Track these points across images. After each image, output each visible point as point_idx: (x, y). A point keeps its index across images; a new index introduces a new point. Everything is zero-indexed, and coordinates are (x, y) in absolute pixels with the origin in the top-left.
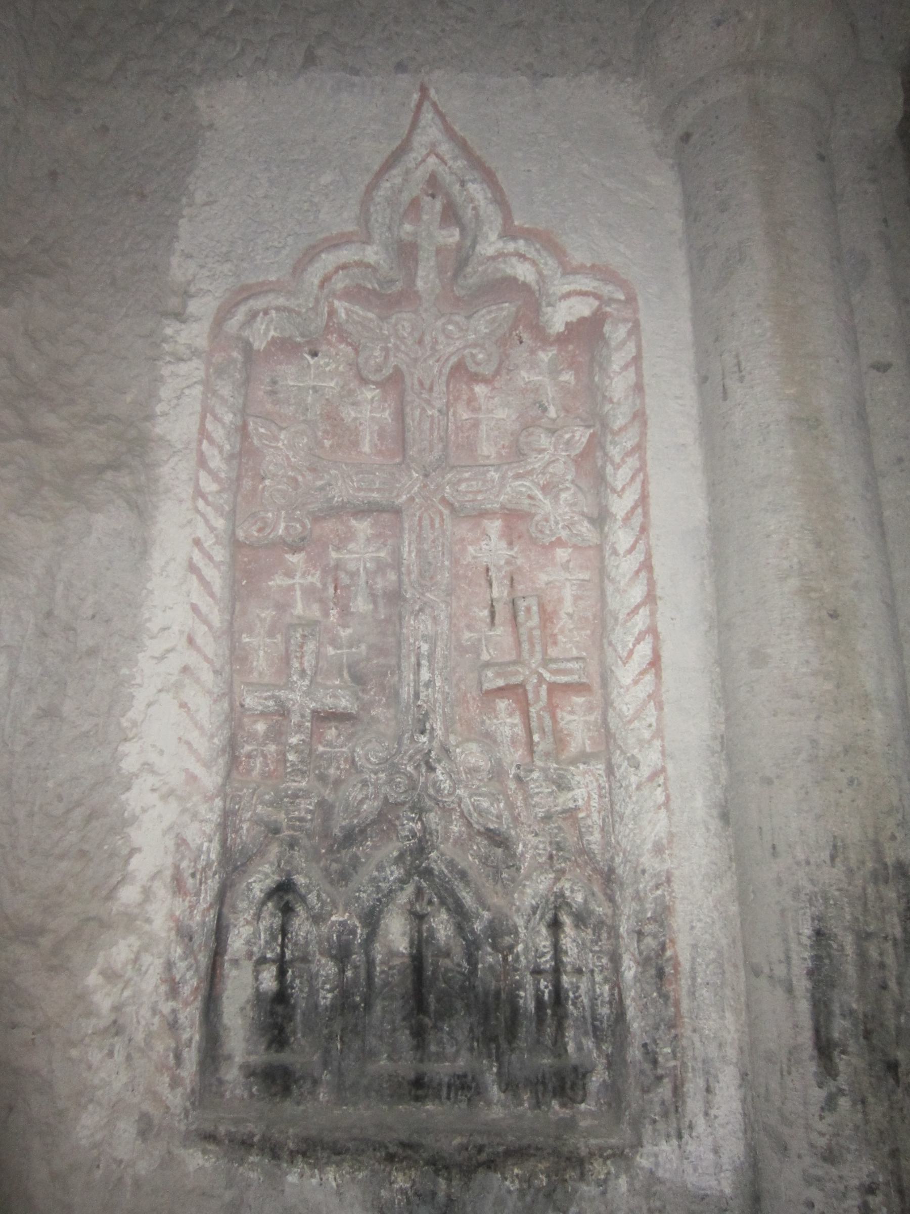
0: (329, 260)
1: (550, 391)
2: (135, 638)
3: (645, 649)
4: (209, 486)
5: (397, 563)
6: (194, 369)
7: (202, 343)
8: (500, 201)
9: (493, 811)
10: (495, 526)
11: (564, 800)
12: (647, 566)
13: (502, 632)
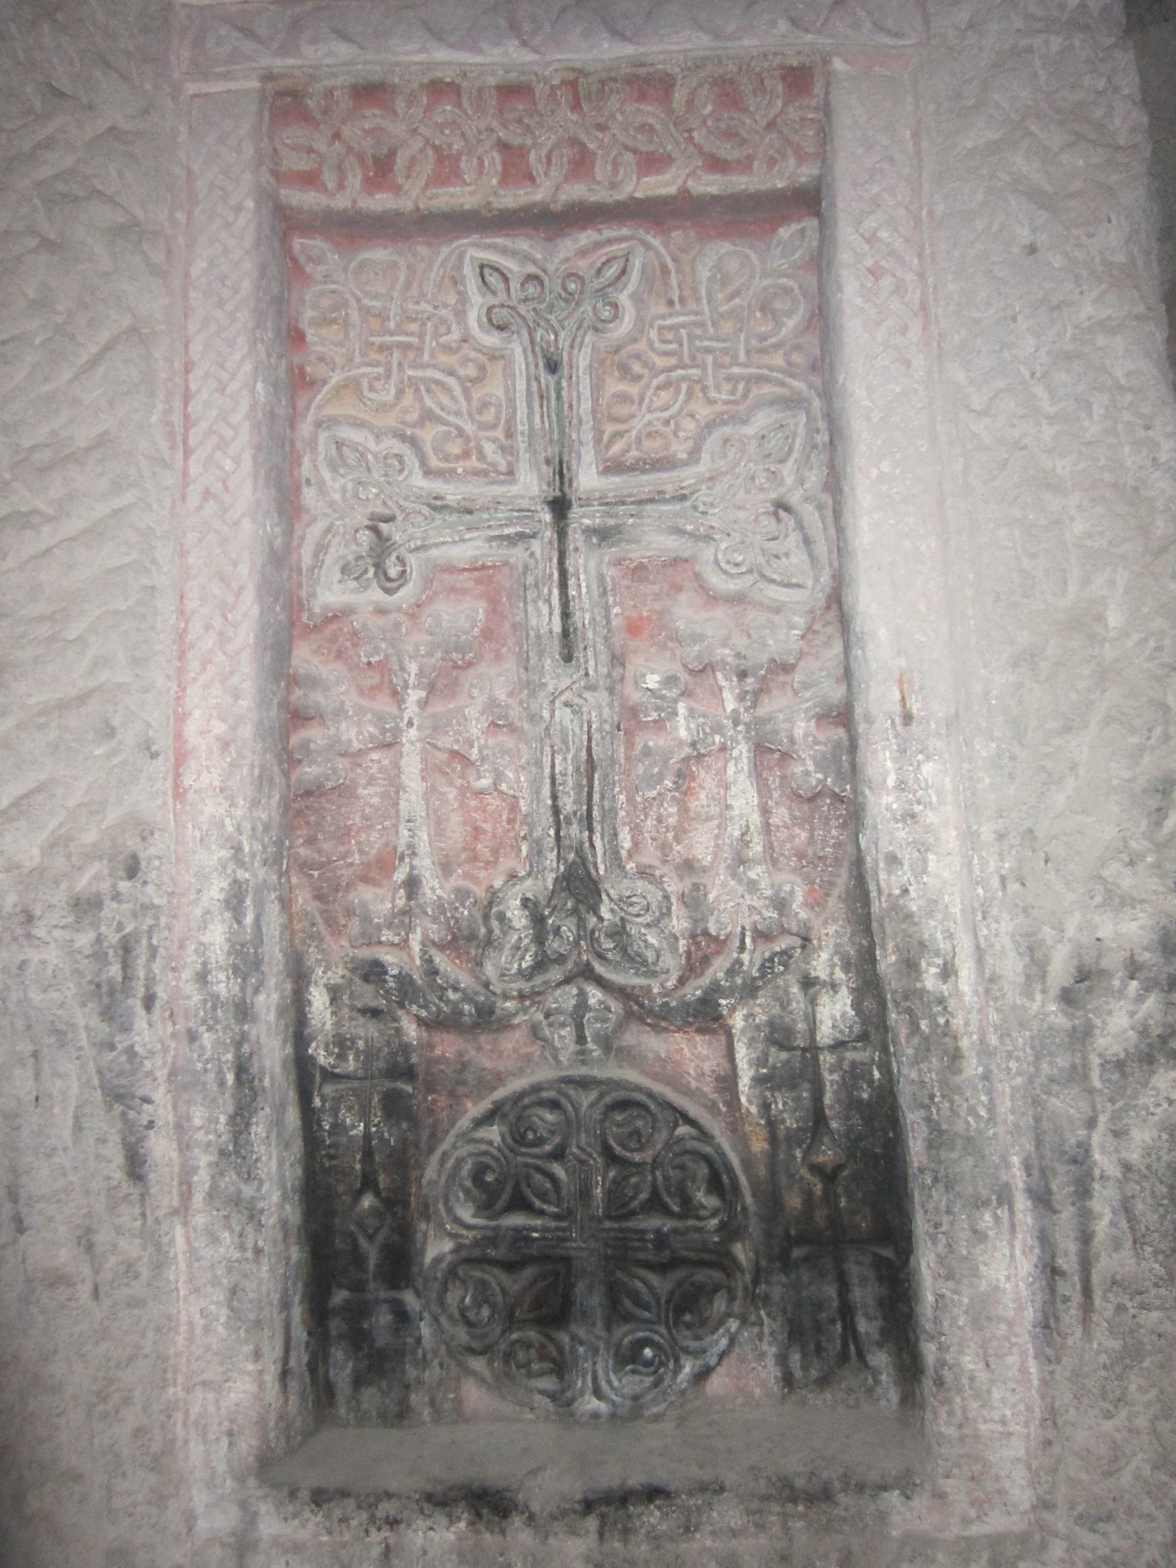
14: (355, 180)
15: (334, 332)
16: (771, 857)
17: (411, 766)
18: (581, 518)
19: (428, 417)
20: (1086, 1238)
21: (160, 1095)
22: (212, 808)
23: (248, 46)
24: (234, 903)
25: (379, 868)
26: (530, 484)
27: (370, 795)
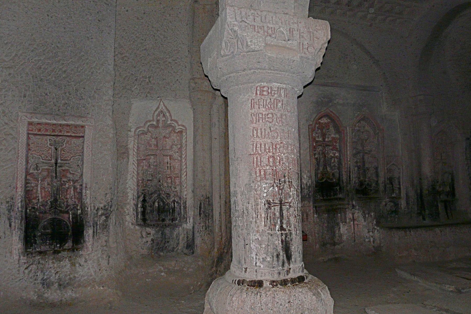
0: (149, 124)
1: (176, 140)
2: (127, 172)
3: (185, 173)
4: (135, 153)
5: (156, 162)
6: (133, 139)
7: (133, 135)
8: (170, 115)
9: (168, 191)
10: (168, 158)
11: (176, 190)
12: (186, 164)
13: (169, 170)
14: (37, 131)
15: (33, 145)
16: (75, 198)
17: (39, 189)
18: (58, 165)
19: (43, 154)
20: (97, 229)
21: (13, 219)
22: (20, 193)
23: (26, 118)
24: (21, 202)
25: (35, 198)
26: (53, 161)
27: (35, 191)
